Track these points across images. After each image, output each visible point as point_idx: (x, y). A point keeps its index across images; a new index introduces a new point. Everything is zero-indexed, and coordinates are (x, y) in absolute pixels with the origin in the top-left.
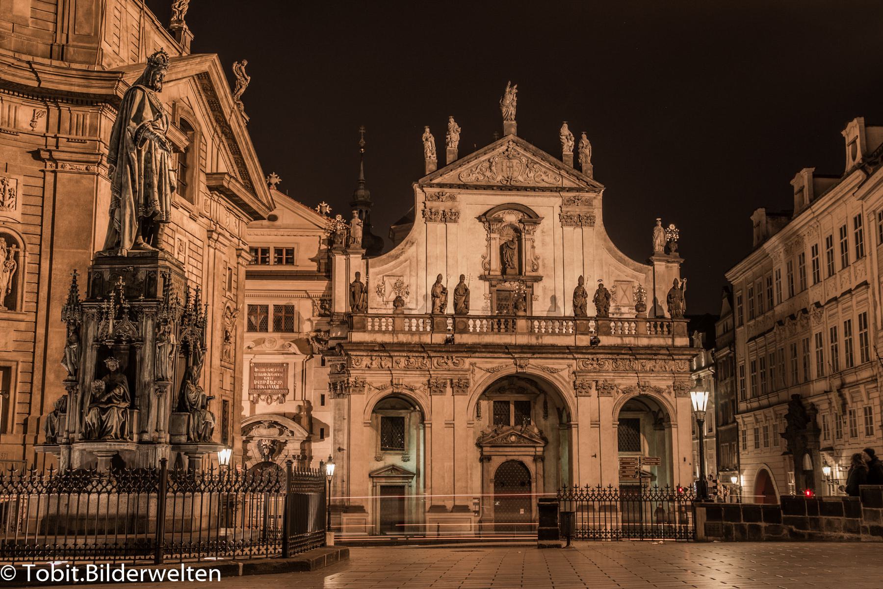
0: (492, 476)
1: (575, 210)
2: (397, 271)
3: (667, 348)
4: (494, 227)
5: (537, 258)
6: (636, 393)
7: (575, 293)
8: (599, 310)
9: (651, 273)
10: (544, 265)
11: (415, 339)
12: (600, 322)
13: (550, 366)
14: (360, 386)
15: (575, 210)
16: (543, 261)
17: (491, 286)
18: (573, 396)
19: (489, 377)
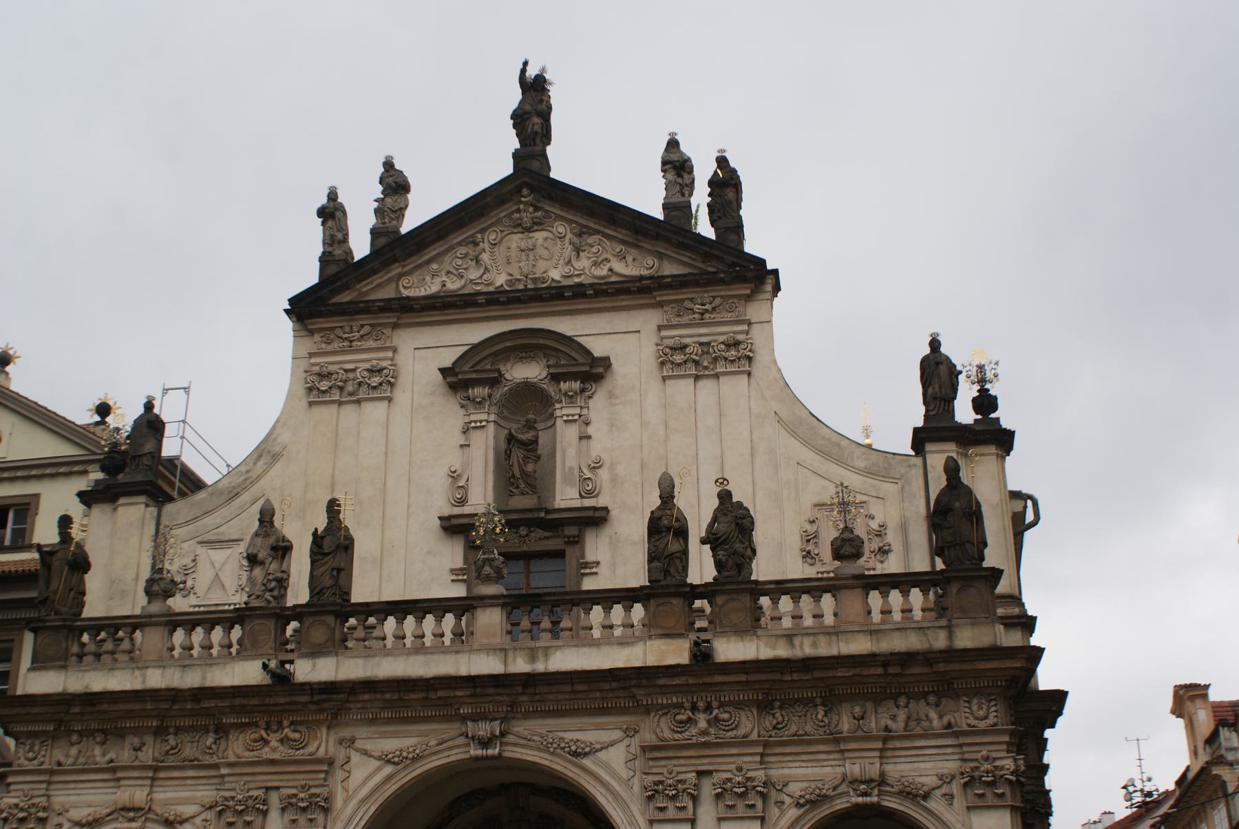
1: (691, 336)
2: (231, 530)
3: (927, 657)
4: (479, 392)
6: (840, 804)
8: (719, 565)
9: (917, 473)
10: (614, 480)
11: (191, 679)
12: (720, 600)
13: (568, 736)
15: (691, 336)
16: (612, 467)
17: (471, 547)
18: (642, 822)
19: (389, 778)
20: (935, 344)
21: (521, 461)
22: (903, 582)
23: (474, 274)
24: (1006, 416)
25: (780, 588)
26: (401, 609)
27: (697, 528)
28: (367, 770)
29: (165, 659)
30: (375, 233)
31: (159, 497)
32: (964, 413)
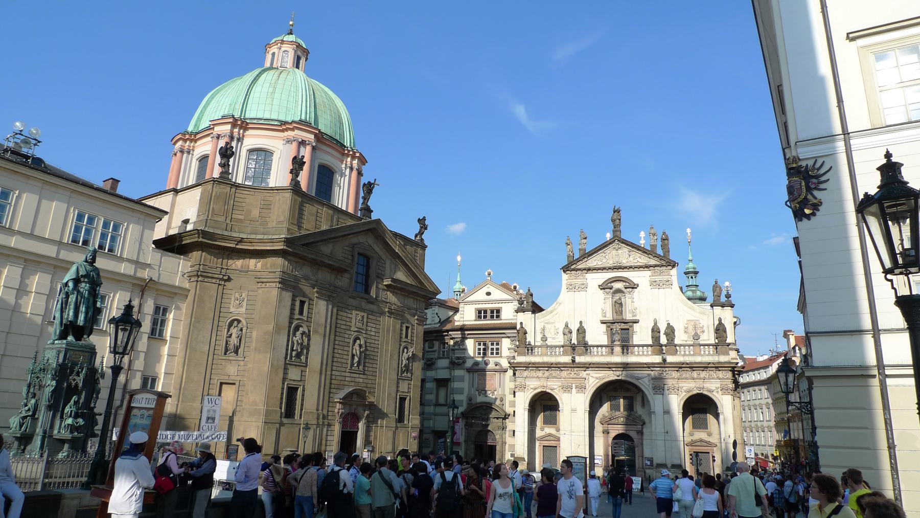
0: (610, 440)
1: (658, 278)
5: (636, 309)
6: (695, 392)
7: (653, 330)
14: (523, 387)
15: (658, 278)
20: (716, 282)
21: (618, 306)
22: (709, 345)
23: (604, 261)
24: (733, 300)
25: (680, 346)
26: (598, 346)
27: (662, 332)
28: (594, 380)
29: (546, 355)
30: (580, 250)
31: (534, 312)
32: (723, 299)
